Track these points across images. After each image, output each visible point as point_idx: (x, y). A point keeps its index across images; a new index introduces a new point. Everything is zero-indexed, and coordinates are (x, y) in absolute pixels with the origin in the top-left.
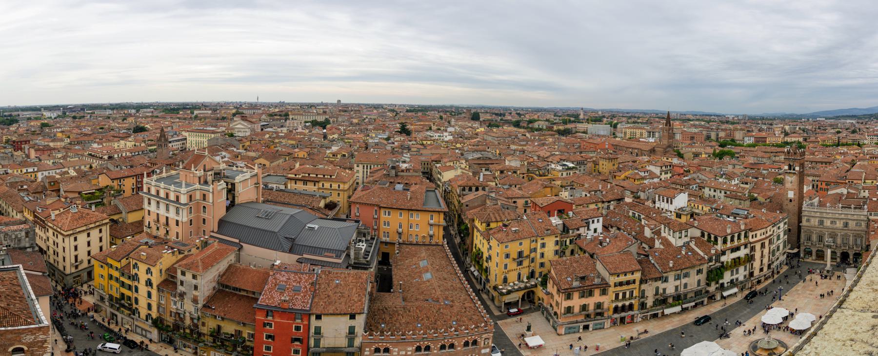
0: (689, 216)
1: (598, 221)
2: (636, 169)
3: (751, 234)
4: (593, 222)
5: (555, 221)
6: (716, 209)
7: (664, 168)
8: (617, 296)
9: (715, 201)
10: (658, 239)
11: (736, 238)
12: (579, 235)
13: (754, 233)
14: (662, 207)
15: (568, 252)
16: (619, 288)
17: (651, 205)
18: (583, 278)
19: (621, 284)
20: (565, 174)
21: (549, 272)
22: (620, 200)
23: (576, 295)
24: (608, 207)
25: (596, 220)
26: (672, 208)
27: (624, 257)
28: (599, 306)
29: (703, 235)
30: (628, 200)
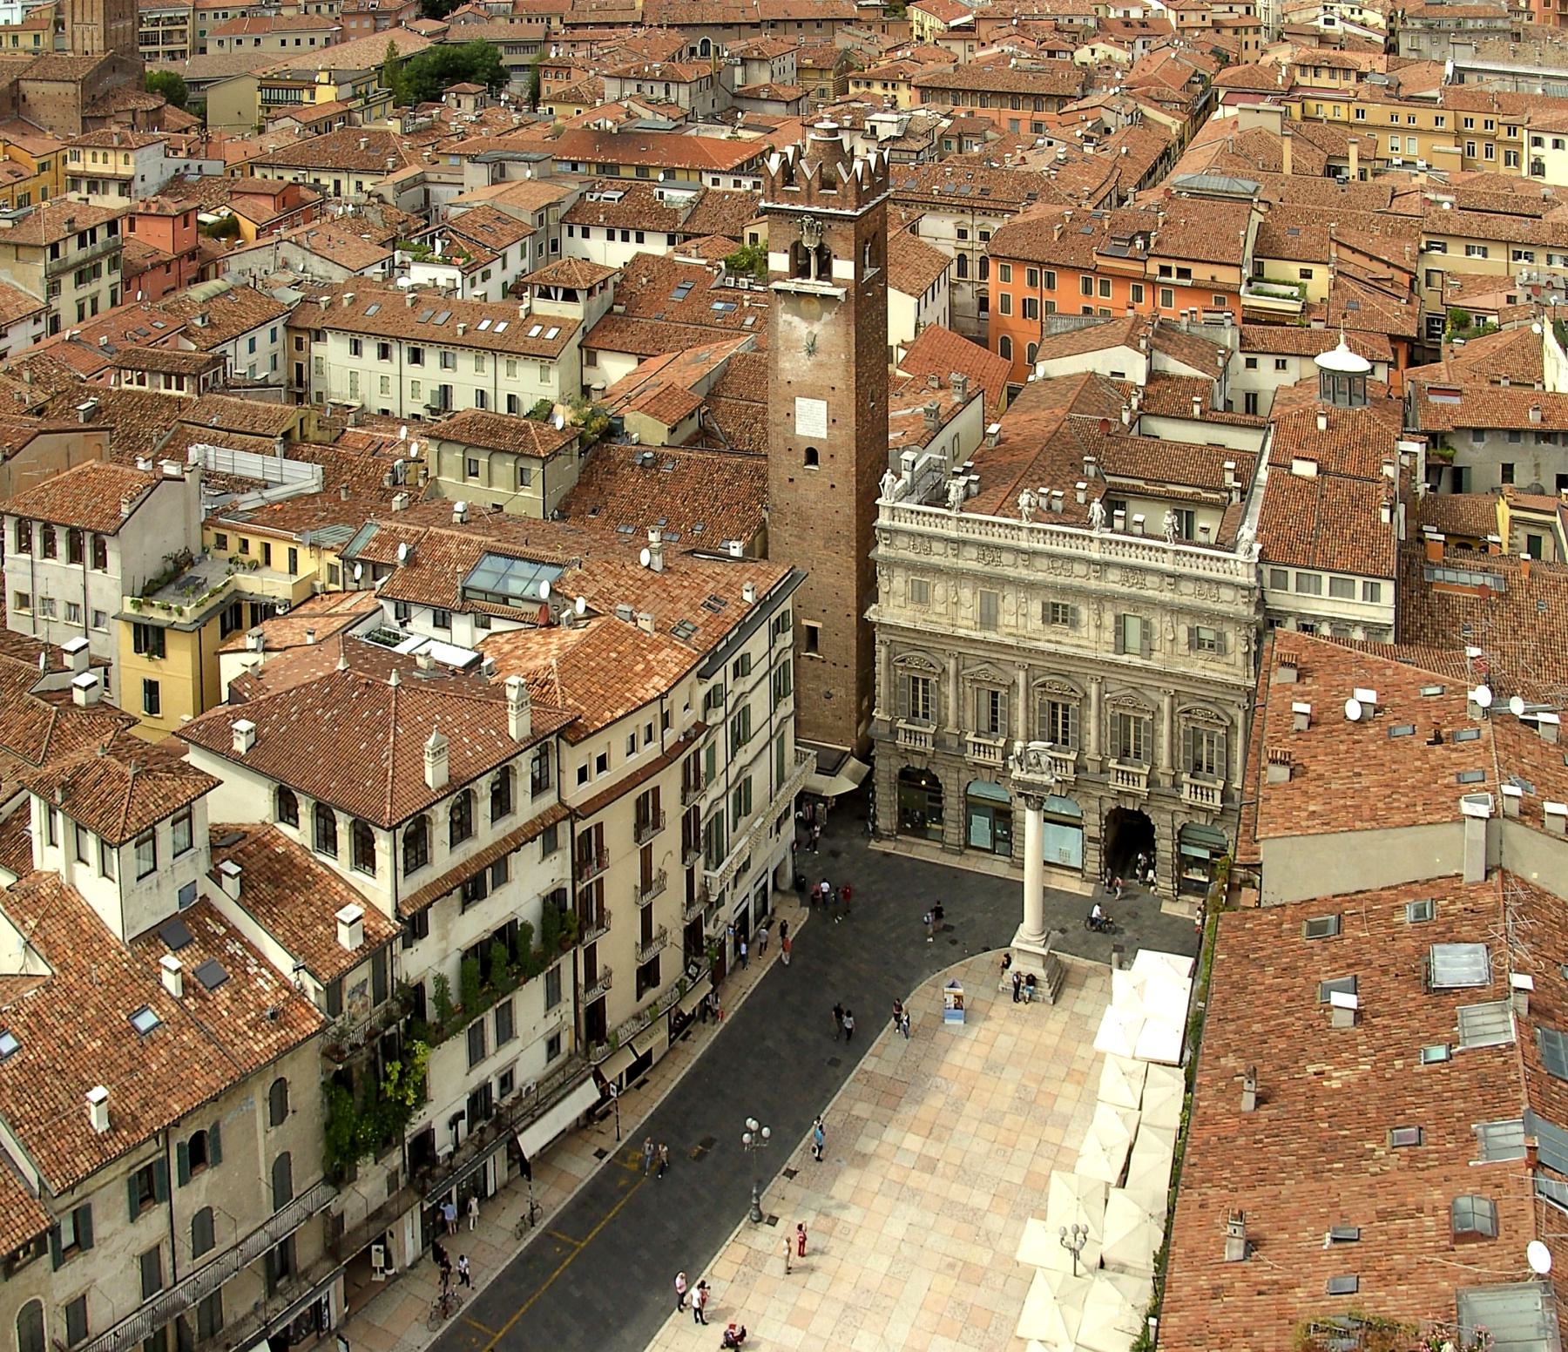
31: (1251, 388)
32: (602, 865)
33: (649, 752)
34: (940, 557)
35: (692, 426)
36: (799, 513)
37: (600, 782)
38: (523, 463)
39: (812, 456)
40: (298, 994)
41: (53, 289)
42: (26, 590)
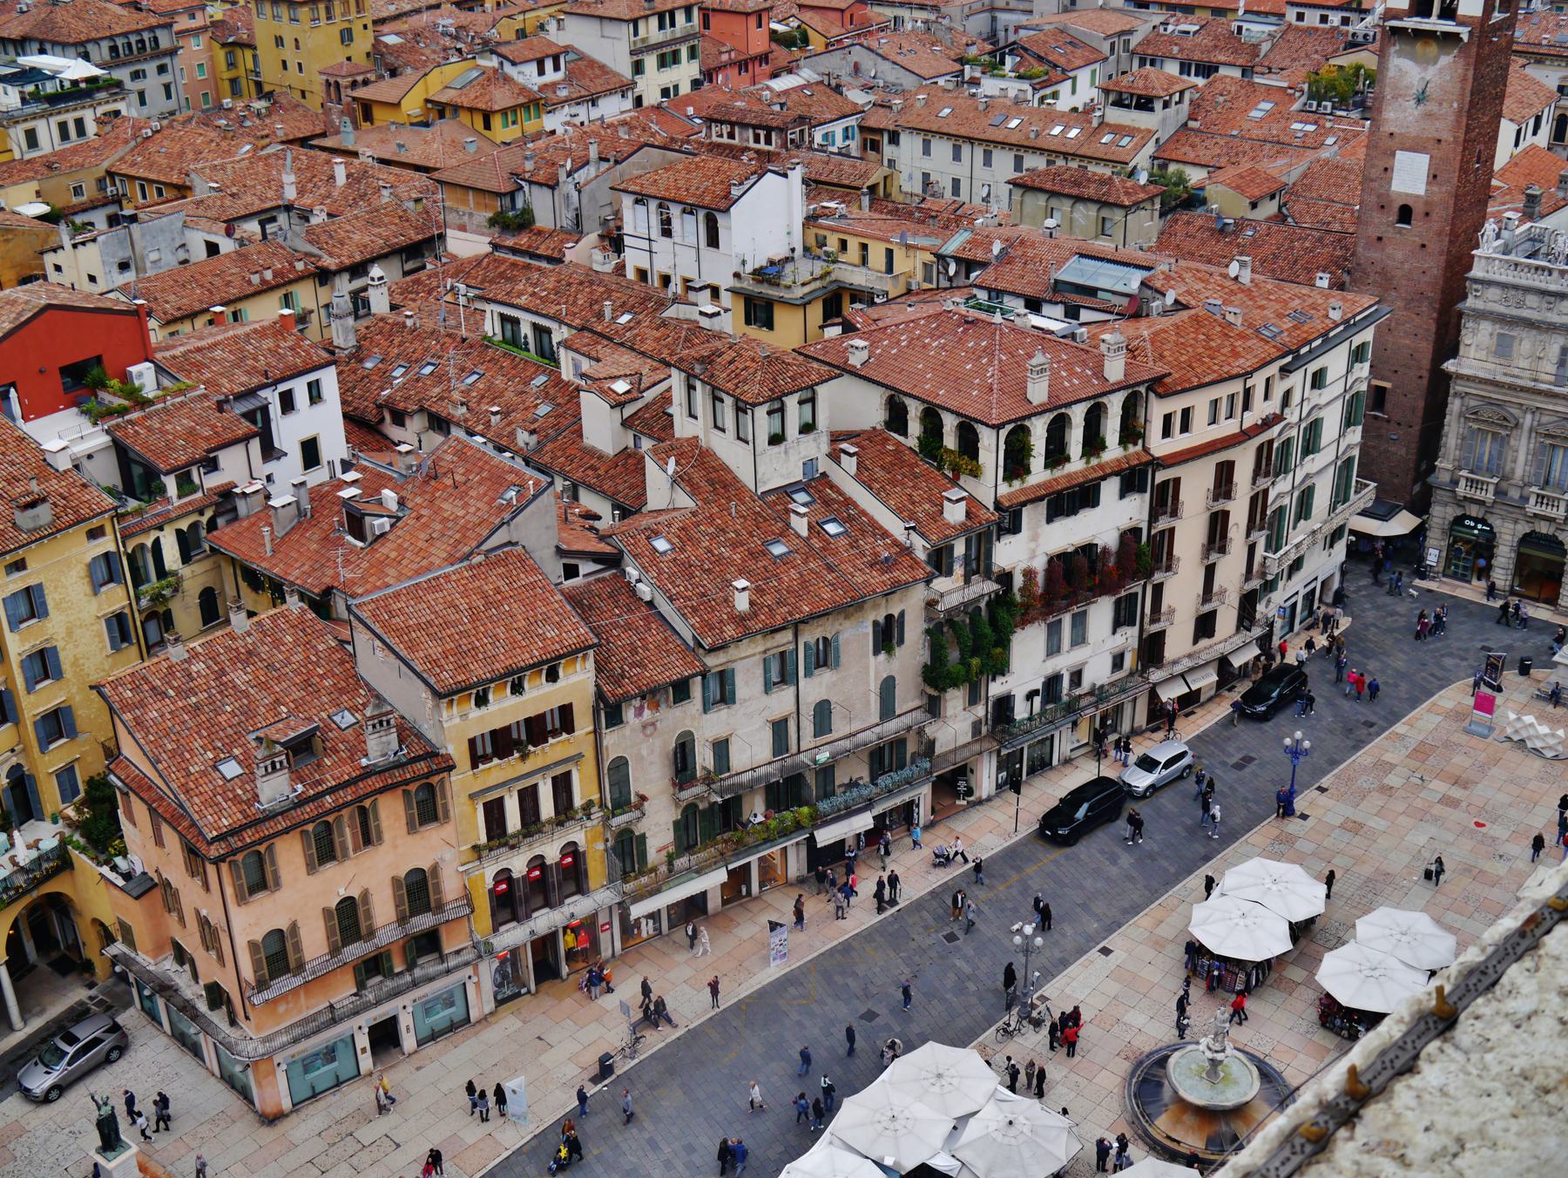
0: (816, 312)
1: (315, 395)
2: (489, 47)
3: (1158, 409)
4: (287, 402)
5: (66, 435)
6: (968, 265)
7: (651, 31)
8: (494, 812)
9: (957, 218)
10: (661, 458)
11: (1075, 439)
12: (227, 496)
13: (1175, 405)
14: (662, 265)
15: (186, 614)
16: (498, 771)
17: (602, 263)
18: (302, 748)
19: (502, 743)
20: (47, 131)
21: (112, 753)
22: (418, 250)
23: (290, 855)
24: (359, 302)
25: (299, 387)
26: (719, 269)
27: (494, 582)
28: (417, 890)
29: (897, 418)
30: (466, 244)
32: (1174, 513)
33: (1228, 427)
34: (1533, 309)
35: (1270, 208)
36: (1383, 273)
37: (1181, 442)
38: (1105, 213)
39: (1405, 214)
40: (907, 551)
41: (638, 68)
42: (645, 265)
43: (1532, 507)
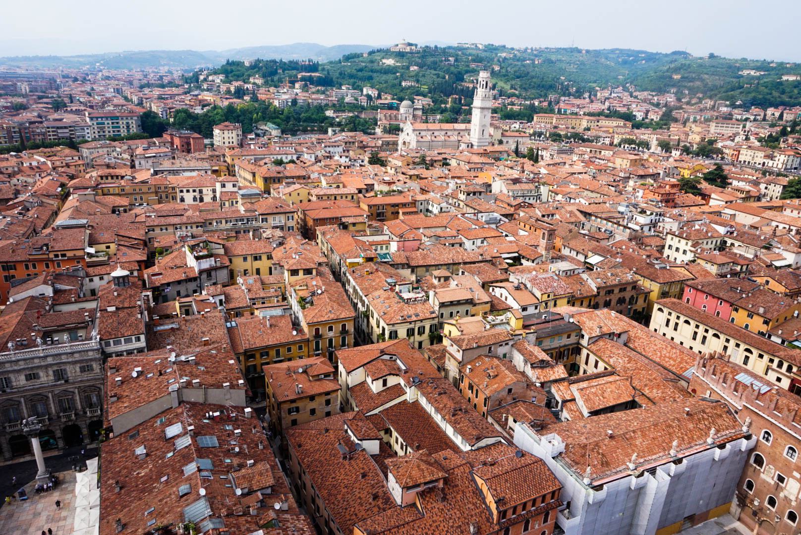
31: (92, 288)
43: (8, 430)
